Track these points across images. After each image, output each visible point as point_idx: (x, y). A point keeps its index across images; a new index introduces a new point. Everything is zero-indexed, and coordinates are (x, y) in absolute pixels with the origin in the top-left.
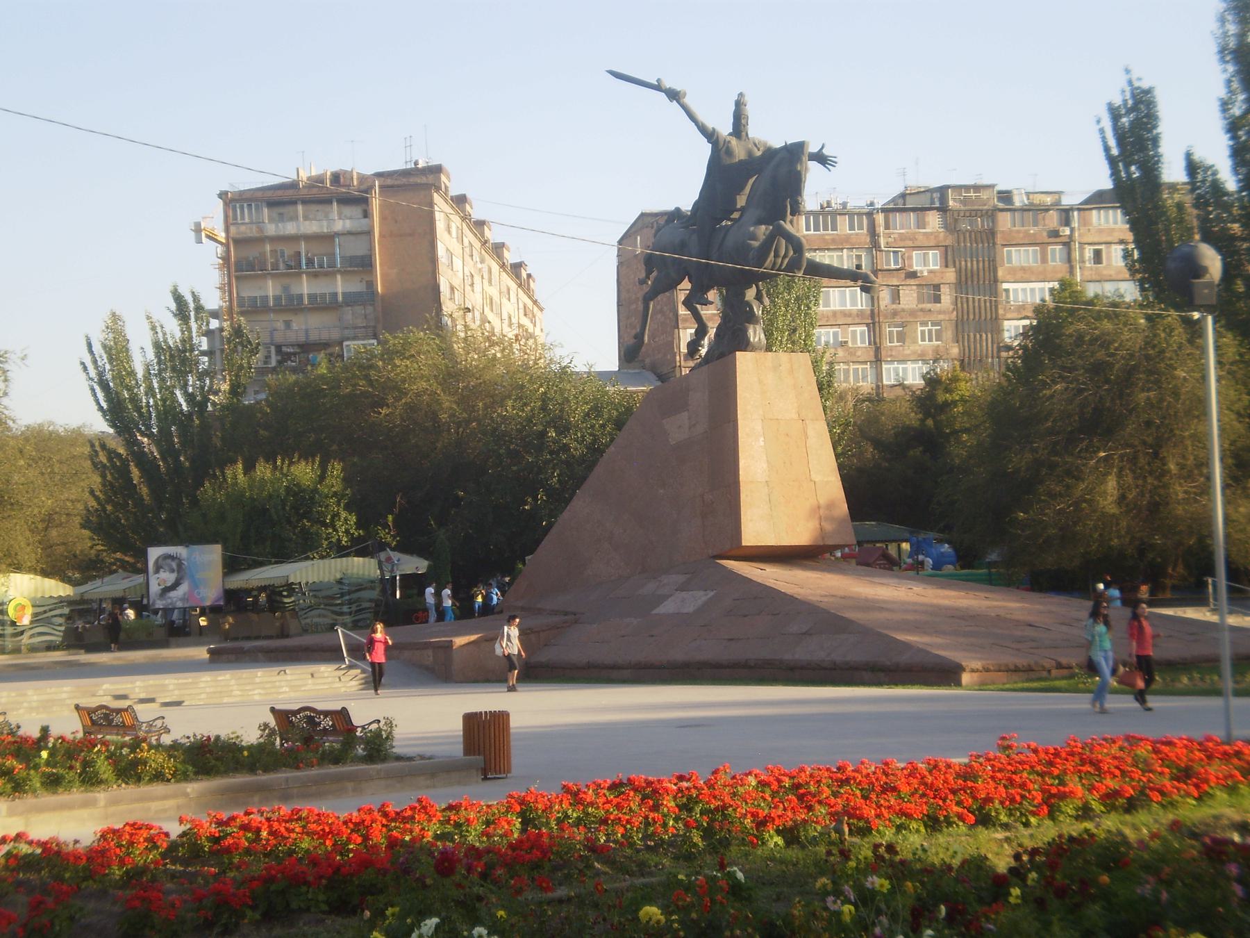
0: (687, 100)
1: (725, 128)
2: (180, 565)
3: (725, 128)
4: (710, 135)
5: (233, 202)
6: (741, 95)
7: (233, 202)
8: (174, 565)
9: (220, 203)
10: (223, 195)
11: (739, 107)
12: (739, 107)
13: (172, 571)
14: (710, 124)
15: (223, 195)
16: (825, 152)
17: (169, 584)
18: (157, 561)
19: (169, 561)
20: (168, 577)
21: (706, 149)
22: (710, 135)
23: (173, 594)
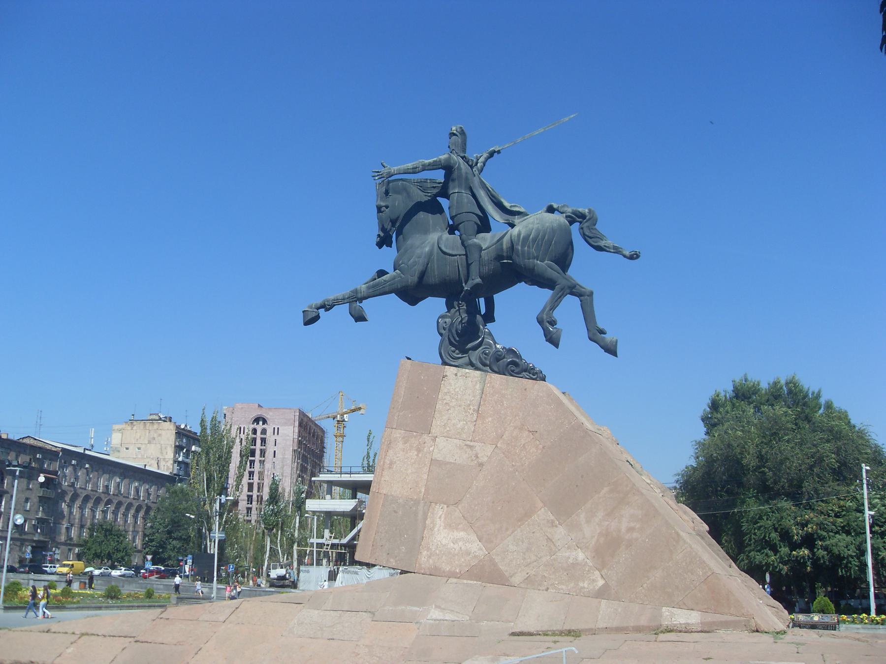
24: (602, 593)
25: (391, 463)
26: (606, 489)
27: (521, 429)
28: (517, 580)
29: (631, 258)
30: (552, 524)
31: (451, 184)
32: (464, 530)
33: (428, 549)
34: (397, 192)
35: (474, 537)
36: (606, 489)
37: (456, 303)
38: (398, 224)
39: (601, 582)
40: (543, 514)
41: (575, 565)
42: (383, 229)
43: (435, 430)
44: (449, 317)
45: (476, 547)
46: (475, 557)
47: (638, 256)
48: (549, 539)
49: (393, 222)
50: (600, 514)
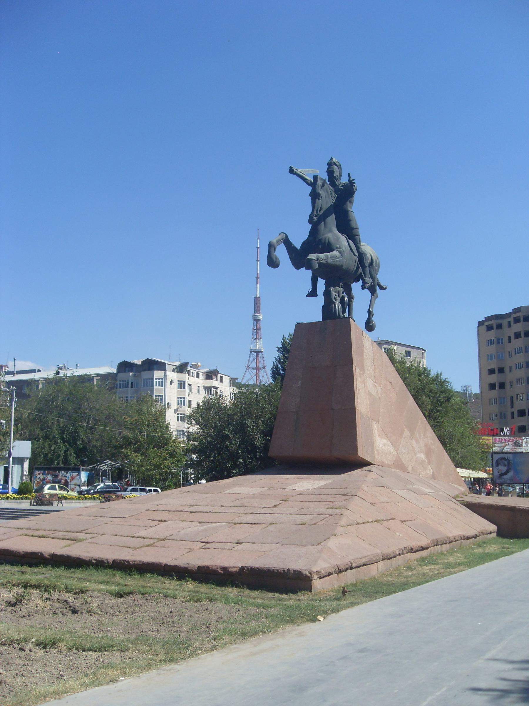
2: (509, 463)
8: (506, 463)
11: (330, 164)
13: (505, 466)
17: (503, 472)
18: (497, 461)
19: (503, 461)
20: (503, 469)
23: (505, 477)
24: (433, 477)
25: (359, 390)
26: (420, 422)
27: (386, 378)
28: (410, 469)
29: (381, 288)
30: (411, 439)
31: (348, 203)
32: (385, 439)
33: (377, 450)
34: (324, 190)
35: (390, 444)
36: (420, 422)
37: (341, 284)
38: (321, 213)
39: (432, 471)
40: (407, 433)
41: (423, 461)
42: (317, 212)
43: (366, 372)
44: (335, 292)
45: (391, 449)
46: (394, 455)
47: (386, 289)
48: (412, 447)
49: (321, 209)
50: (422, 434)
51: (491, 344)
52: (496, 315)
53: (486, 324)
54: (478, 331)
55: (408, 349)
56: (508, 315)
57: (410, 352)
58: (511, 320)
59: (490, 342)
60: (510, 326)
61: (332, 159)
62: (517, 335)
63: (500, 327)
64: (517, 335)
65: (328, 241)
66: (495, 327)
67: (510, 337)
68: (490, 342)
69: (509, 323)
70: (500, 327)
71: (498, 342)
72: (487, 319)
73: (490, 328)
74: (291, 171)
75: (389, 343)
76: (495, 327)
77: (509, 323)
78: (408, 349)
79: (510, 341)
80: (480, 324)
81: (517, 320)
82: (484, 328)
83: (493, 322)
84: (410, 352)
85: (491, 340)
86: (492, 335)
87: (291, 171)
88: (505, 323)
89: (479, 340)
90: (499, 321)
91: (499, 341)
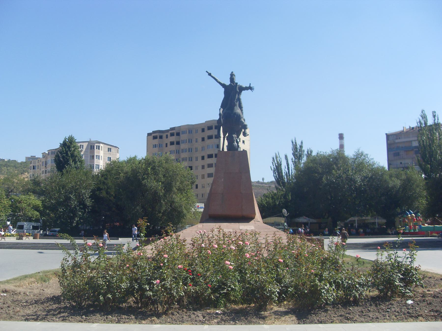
0: (212, 74)
1: (228, 83)
3: (228, 83)
4: (223, 85)
5: (388, 136)
6: (232, 72)
7: (388, 136)
9: (385, 136)
10: (386, 134)
11: (232, 75)
12: (232, 75)
14: (222, 83)
15: (386, 134)
16: (251, 86)
21: (223, 90)
22: (223, 85)
51: (155, 147)
52: (159, 131)
53: (153, 135)
54: (147, 139)
55: (110, 147)
56: (167, 131)
57: (110, 149)
58: (169, 134)
59: (155, 146)
60: (167, 137)
61: (232, 72)
62: (172, 143)
63: (161, 137)
64: (172, 143)
65: (239, 115)
66: (158, 137)
67: (167, 144)
68: (155, 146)
69: (167, 135)
70: (161, 137)
71: (160, 147)
72: (154, 132)
73: (155, 138)
74: (210, 74)
75: (100, 143)
76: (158, 137)
77: (167, 135)
78: (110, 147)
79: (167, 146)
80: (149, 134)
81: (172, 135)
82: (151, 137)
83: (158, 134)
84: (110, 149)
85: (155, 145)
86: (156, 142)
87: (210, 74)
88: (164, 135)
89: (147, 144)
90: (161, 134)
91: (160, 146)
